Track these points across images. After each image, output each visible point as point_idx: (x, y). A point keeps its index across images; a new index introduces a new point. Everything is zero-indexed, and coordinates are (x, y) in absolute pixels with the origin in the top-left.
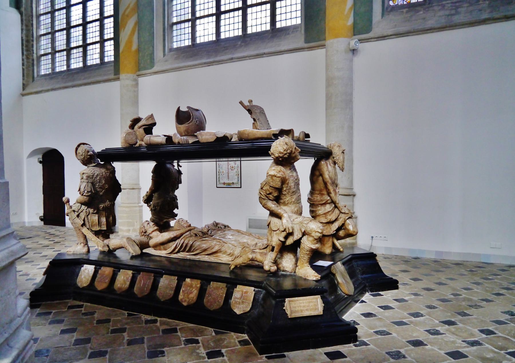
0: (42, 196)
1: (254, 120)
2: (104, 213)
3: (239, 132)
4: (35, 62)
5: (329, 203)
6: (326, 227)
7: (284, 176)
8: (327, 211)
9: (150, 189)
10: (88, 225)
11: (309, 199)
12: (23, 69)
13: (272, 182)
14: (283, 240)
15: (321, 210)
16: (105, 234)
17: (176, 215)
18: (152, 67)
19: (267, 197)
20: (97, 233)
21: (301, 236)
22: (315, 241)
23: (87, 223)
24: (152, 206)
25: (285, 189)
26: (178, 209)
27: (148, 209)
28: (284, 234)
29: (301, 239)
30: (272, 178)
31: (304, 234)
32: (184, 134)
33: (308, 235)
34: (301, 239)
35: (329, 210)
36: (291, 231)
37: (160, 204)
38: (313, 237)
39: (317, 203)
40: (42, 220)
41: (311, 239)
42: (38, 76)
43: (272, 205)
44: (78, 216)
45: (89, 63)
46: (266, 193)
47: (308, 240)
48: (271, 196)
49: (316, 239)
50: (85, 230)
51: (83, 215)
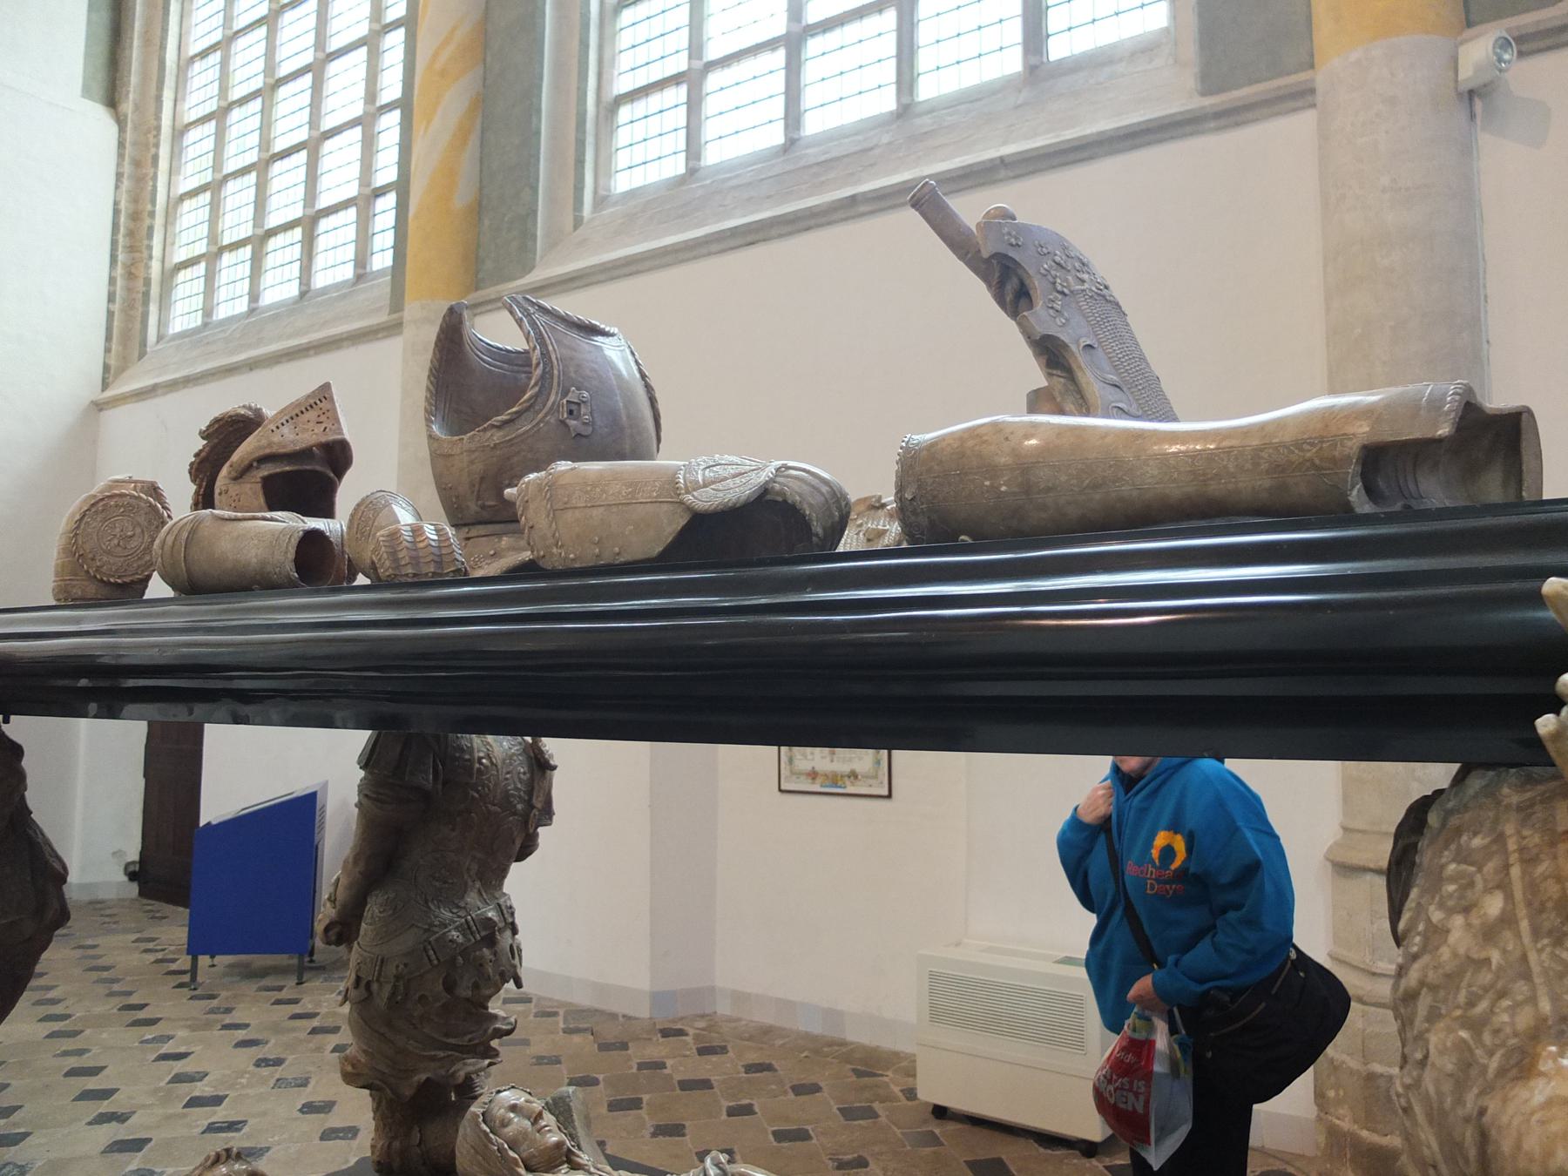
0: (142, 782)
1: (1051, 353)
3: (916, 468)
4: (155, 290)
12: (110, 314)
18: (528, 268)
32: (473, 507)
37: (391, 970)
40: (132, 876)
42: (160, 338)
45: (320, 280)
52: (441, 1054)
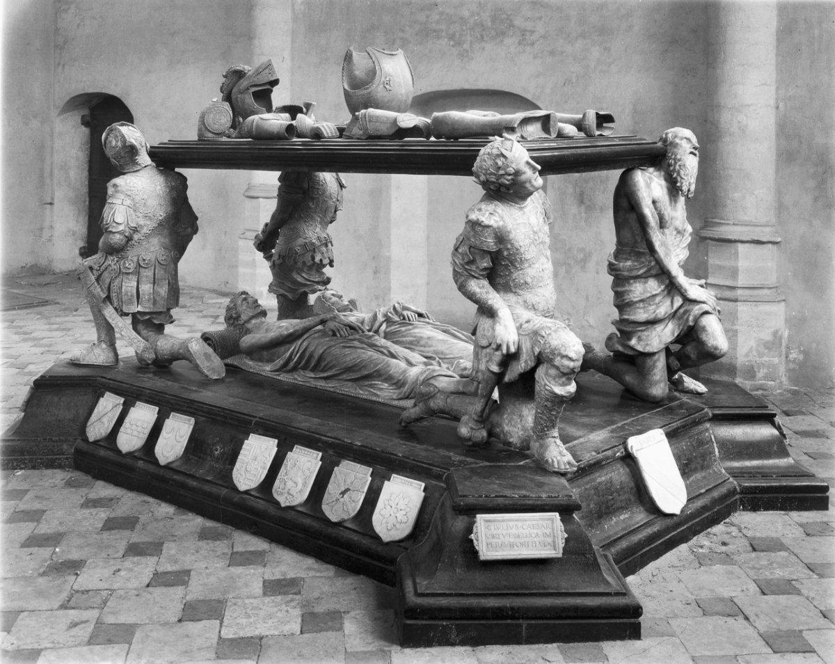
2: (150, 273)
5: (656, 276)
6: (646, 333)
7: (501, 223)
8: (649, 295)
9: (273, 217)
10: (115, 301)
11: (611, 265)
13: (474, 236)
14: (495, 369)
15: (638, 290)
16: (150, 323)
17: (328, 281)
19: (466, 270)
20: (138, 321)
21: (533, 364)
22: (564, 379)
23: (113, 295)
24: (275, 258)
25: (505, 253)
26: (331, 266)
27: (267, 264)
28: (498, 356)
29: (534, 370)
30: (473, 229)
31: (539, 360)
33: (548, 362)
34: (534, 370)
35: (654, 293)
36: (513, 350)
38: (557, 368)
39: (626, 273)
41: (553, 372)
43: (480, 287)
44: (98, 280)
46: (463, 260)
47: (547, 374)
48: (474, 268)
49: (564, 374)
50: (109, 312)
51: (106, 277)
52: (309, 283)
